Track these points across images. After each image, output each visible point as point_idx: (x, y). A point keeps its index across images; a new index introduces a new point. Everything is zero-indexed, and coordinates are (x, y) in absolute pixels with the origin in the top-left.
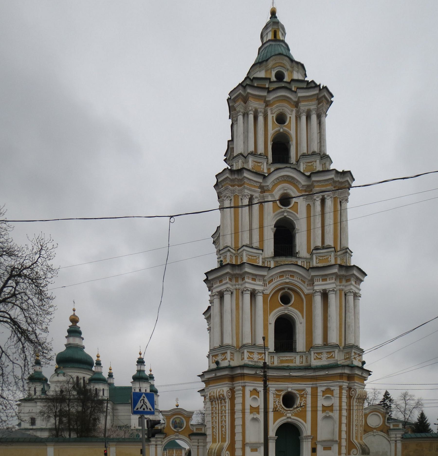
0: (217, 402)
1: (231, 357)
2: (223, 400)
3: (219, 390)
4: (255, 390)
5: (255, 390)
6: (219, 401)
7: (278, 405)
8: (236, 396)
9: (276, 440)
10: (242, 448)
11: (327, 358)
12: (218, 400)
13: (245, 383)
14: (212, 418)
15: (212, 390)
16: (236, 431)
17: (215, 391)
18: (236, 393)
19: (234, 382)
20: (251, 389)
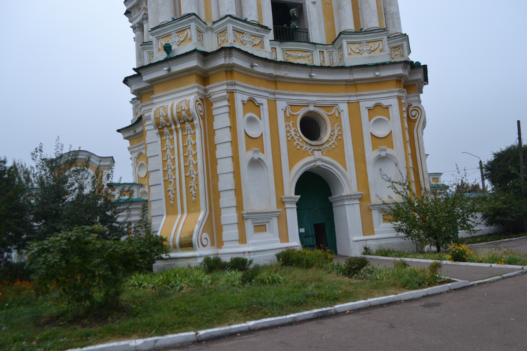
0: (173, 127)
1: (199, 38)
2: (187, 123)
3: (176, 102)
4: (251, 100)
5: (251, 100)
6: (179, 126)
7: (294, 136)
8: (215, 112)
9: (297, 204)
10: (238, 223)
11: (369, 52)
12: (175, 124)
13: (235, 84)
14: (164, 162)
15: (161, 105)
16: (221, 186)
17: (170, 104)
18: (215, 106)
19: (209, 84)
20: (246, 98)
